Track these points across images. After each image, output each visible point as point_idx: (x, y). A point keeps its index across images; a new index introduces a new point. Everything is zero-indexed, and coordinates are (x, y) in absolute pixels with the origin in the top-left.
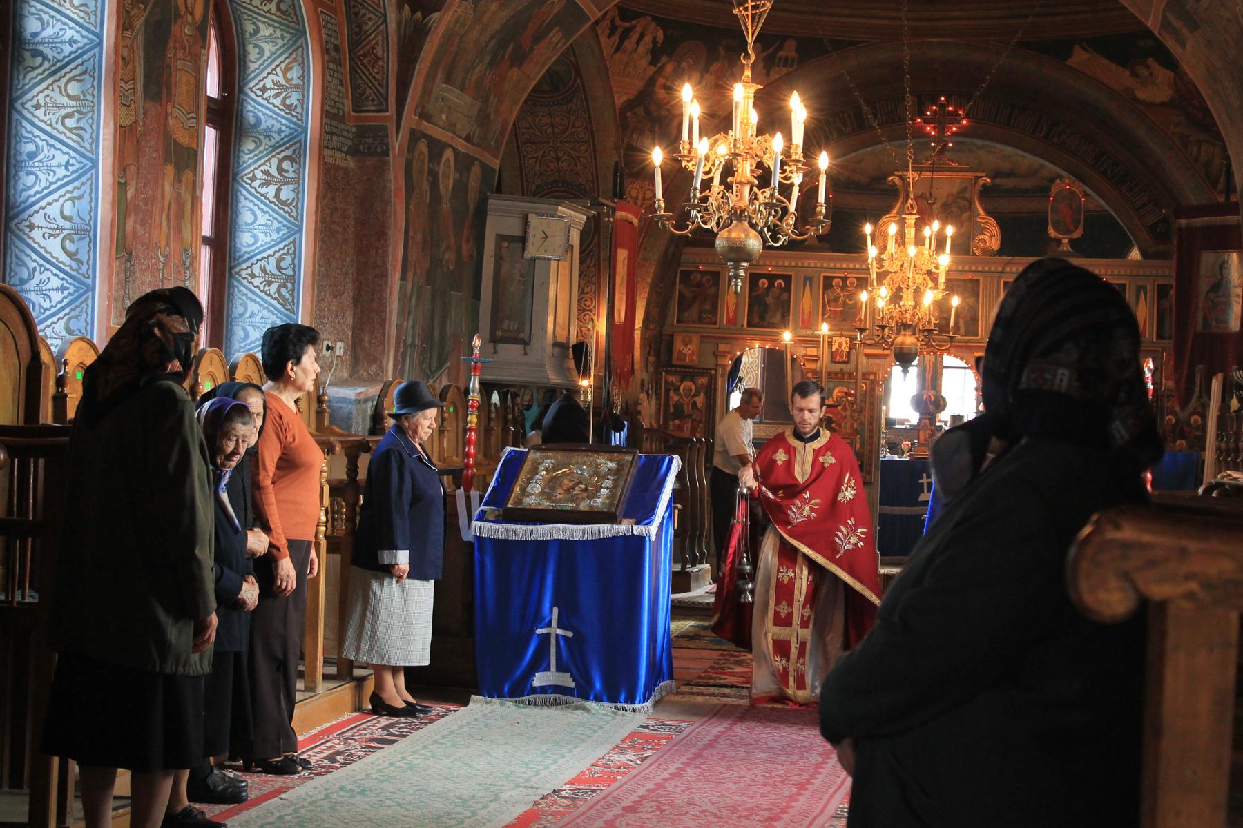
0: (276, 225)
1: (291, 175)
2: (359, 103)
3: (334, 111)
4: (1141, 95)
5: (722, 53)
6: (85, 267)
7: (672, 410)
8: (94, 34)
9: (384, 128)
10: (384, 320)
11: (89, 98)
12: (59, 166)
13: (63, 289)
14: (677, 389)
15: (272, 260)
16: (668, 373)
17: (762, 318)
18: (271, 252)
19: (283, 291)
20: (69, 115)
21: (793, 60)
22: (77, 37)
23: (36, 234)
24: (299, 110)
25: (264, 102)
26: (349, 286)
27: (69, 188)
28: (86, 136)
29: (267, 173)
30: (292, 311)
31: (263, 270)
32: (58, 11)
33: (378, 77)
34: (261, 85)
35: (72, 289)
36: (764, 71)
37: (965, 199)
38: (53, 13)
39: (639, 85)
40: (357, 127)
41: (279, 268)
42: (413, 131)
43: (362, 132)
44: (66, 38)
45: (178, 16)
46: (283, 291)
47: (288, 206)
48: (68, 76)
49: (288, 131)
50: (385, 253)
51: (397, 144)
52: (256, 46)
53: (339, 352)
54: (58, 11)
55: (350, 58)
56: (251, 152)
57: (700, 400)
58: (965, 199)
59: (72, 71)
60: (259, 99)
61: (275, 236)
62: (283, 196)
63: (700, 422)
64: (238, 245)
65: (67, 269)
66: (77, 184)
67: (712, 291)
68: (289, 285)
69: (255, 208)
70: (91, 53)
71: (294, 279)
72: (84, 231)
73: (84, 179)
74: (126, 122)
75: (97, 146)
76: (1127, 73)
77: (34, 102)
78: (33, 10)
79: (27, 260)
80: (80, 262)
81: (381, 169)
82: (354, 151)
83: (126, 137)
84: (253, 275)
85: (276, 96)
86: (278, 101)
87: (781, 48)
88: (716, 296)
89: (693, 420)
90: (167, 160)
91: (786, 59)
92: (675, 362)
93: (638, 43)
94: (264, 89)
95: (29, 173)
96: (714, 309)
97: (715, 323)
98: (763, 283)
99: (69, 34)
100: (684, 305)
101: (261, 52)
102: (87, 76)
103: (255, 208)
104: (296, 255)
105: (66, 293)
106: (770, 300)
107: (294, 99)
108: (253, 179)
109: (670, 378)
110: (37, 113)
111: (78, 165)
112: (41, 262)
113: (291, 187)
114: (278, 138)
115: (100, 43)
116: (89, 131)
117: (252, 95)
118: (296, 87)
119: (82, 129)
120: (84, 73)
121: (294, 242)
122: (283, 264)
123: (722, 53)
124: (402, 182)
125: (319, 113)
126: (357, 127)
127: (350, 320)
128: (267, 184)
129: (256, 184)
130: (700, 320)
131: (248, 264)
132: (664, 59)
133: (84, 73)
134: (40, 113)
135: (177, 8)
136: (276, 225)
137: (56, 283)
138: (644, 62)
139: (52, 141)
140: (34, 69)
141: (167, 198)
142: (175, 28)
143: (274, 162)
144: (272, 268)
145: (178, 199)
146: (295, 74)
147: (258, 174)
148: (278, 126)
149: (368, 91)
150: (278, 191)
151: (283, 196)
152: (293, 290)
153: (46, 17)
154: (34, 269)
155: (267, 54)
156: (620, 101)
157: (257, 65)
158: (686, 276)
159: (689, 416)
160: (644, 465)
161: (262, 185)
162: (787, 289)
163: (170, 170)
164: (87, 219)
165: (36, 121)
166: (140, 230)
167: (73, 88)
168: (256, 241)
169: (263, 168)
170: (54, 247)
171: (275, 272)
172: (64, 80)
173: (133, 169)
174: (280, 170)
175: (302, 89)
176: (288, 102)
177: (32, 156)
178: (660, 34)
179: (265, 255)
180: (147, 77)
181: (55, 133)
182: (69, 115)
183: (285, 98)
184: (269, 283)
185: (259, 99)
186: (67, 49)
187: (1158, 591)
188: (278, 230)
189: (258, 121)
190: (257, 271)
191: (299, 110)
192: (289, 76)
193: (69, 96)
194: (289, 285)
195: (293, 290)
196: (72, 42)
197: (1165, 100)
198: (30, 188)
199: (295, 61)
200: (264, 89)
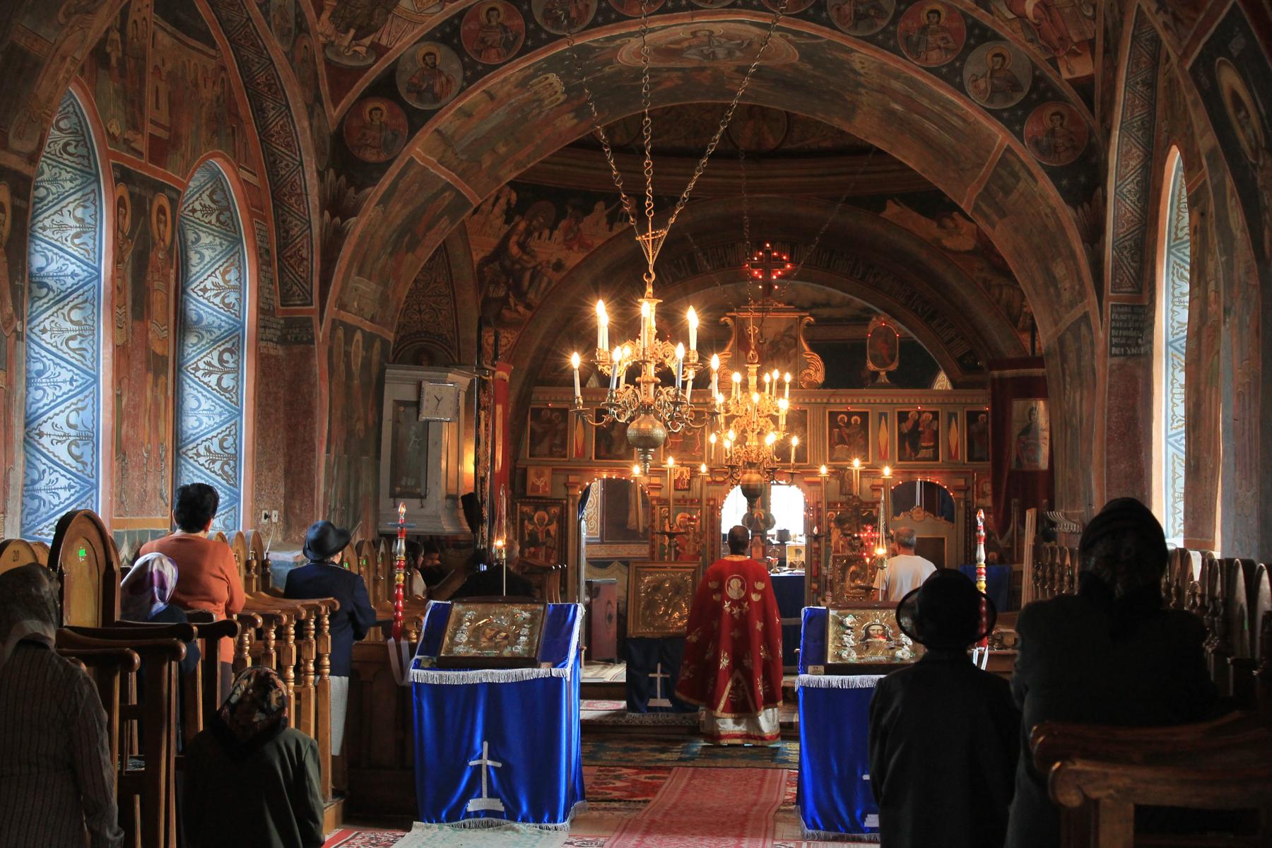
0: (218, 409)
1: (231, 365)
2: (286, 299)
3: (266, 307)
4: (948, 243)
5: (570, 211)
6: (89, 468)
7: (527, 538)
8: (93, 268)
9: (310, 320)
10: (313, 490)
11: (90, 323)
12: (65, 382)
13: (70, 487)
14: (531, 519)
15: (216, 441)
16: (522, 504)
17: (609, 450)
18: (214, 433)
19: (226, 468)
20: (73, 338)
22: (78, 271)
23: (45, 441)
24: (237, 308)
25: (205, 301)
26: (281, 460)
27: (74, 400)
28: (88, 356)
29: (209, 364)
30: (235, 486)
31: (207, 449)
32: (61, 249)
33: (304, 275)
34: (202, 286)
35: (78, 488)
37: (791, 337)
38: (56, 250)
39: (495, 241)
40: (285, 319)
41: (222, 448)
42: (334, 321)
43: (290, 323)
44: (69, 272)
45: (154, 244)
46: (226, 468)
47: (229, 392)
48: (71, 304)
49: (227, 327)
50: (313, 430)
51: (320, 334)
52: (197, 252)
53: (275, 519)
54: (61, 249)
55: (279, 259)
56: (194, 345)
57: (553, 528)
58: (791, 337)
59: (74, 300)
60: (201, 299)
61: (218, 419)
62: (224, 384)
64: (185, 428)
65: (74, 470)
66: (80, 397)
67: (561, 427)
68: (232, 462)
69: (199, 395)
70: (90, 285)
71: (236, 457)
72: (88, 437)
73: (86, 393)
74: (120, 342)
75: (98, 365)
76: (935, 225)
77: (41, 327)
78: (38, 248)
79: (37, 463)
80: (84, 464)
81: (307, 356)
82: (282, 341)
83: (122, 354)
84: (198, 455)
85: (216, 295)
86: (217, 300)
88: (566, 429)
90: (148, 370)
92: (529, 493)
93: (494, 205)
94: (205, 290)
95: (37, 388)
96: (564, 445)
97: (565, 456)
99: (71, 268)
100: (536, 440)
101: (202, 257)
102: (87, 305)
103: (199, 395)
104: (237, 436)
105: (73, 491)
107: (232, 298)
108: (197, 369)
109: (525, 509)
110: (44, 336)
111: (81, 381)
112: (50, 464)
113: (232, 376)
114: (218, 333)
115: (99, 277)
116: (91, 351)
117: (194, 295)
118: (234, 288)
119: (84, 349)
120: (85, 301)
121: (235, 424)
122: (225, 445)
123: (570, 211)
124: (326, 367)
125: (255, 310)
126: (285, 319)
127: (282, 490)
128: (210, 373)
129: (199, 374)
130: (551, 454)
131: (194, 444)
132: (517, 219)
133: (85, 301)
134: (46, 336)
135: (153, 238)
136: (218, 409)
137: (63, 482)
138: (499, 222)
139: (58, 361)
140: (40, 298)
141: (149, 401)
142: (151, 254)
143: (216, 354)
144: (215, 448)
145: (155, 398)
146: (232, 276)
147: (201, 365)
148: (218, 322)
149: (295, 288)
150: (220, 380)
151: (224, 384)
152: (235, 467)
153: (50, 254)
154: (44, 471)
155: (207, 259)
156: (477, 258)
157: (198, 269)
158: (537, 413)
159: (544, 544)
160: (553, 612)
161: (205, 375)
163: (150, 377)
164: (90, 426)
165: (43, 343)
166: (131, 433)
167: (76, 315)
168: (201, 424)
169: (205, 359)
170: (61, 451)
171: (219, 451)
172: (67, 308)
173: (126, 381)
174: (221, 361)
175: (239, 289)
176: (227, 301)
177: (40, 373)
178: (514, 196)
179: (209, 436)
180: (134, 301)
181: (60, 353)
182: (73, 338)
183: (224, 298)
184: (214, 462)
185: (201, 299)
186: (70, 281)
187: (1095, 794)
188: (220, 414)
189: (200, 318)
190: (202, 451)
191: (237, 308)
192: (227, 277)
193: (72, 322)
194: (232, 462)
195: (235, 467)
196: (73, 275)
198: (39, 401)
199: (232, 264)
200: (205, 290)
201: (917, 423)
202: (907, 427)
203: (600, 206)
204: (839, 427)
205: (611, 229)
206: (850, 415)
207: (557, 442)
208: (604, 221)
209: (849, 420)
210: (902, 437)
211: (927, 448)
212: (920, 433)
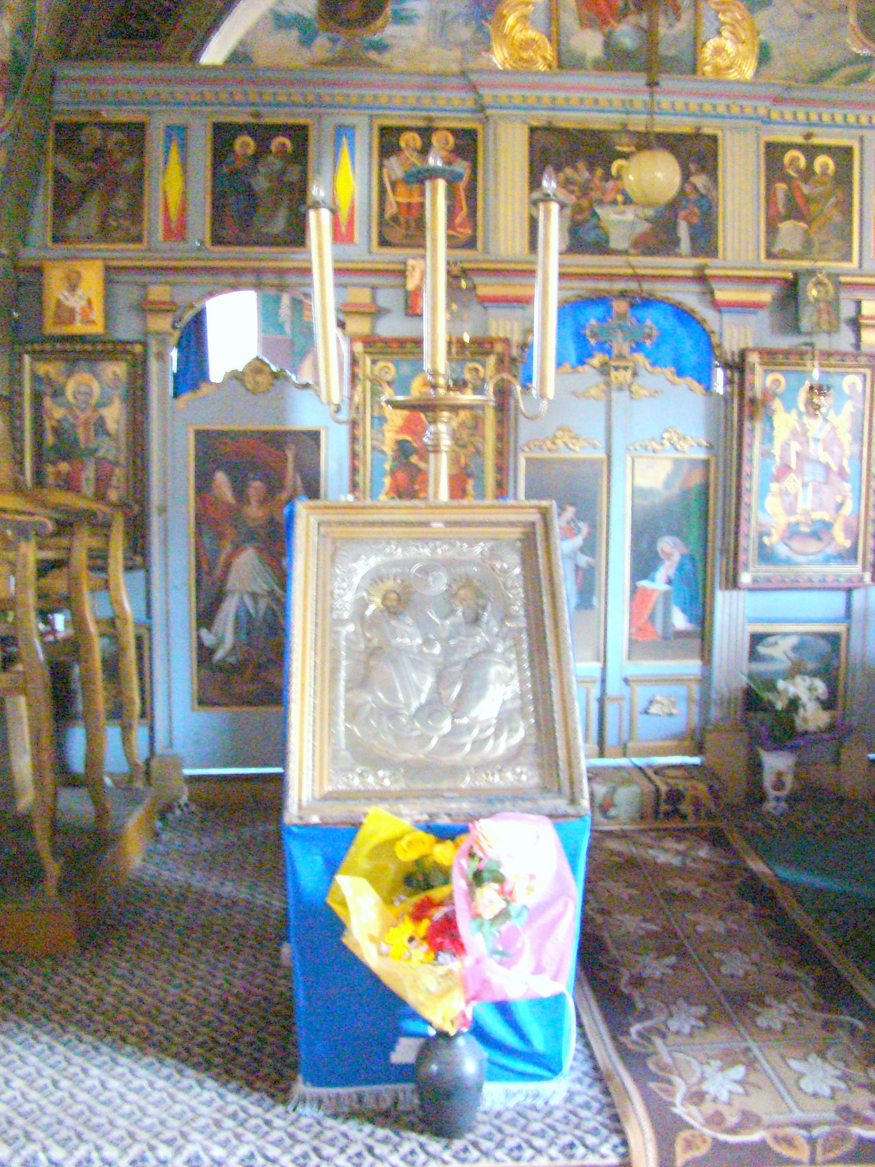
7: (50, 439)
14: (58, 393)
16: (39, 356)
17: (247, 224)
63: (116, 464)
67: (130, 167)
89: (99, 461)
92: (51, 328)
96: (135, 212)
97: (138, 239)
98: (245, 144)
106: (261, 183)
109: (43, 368)
130: (105, 233)
204: (786, 179)
206: (811, 152)
207: (121, 202)
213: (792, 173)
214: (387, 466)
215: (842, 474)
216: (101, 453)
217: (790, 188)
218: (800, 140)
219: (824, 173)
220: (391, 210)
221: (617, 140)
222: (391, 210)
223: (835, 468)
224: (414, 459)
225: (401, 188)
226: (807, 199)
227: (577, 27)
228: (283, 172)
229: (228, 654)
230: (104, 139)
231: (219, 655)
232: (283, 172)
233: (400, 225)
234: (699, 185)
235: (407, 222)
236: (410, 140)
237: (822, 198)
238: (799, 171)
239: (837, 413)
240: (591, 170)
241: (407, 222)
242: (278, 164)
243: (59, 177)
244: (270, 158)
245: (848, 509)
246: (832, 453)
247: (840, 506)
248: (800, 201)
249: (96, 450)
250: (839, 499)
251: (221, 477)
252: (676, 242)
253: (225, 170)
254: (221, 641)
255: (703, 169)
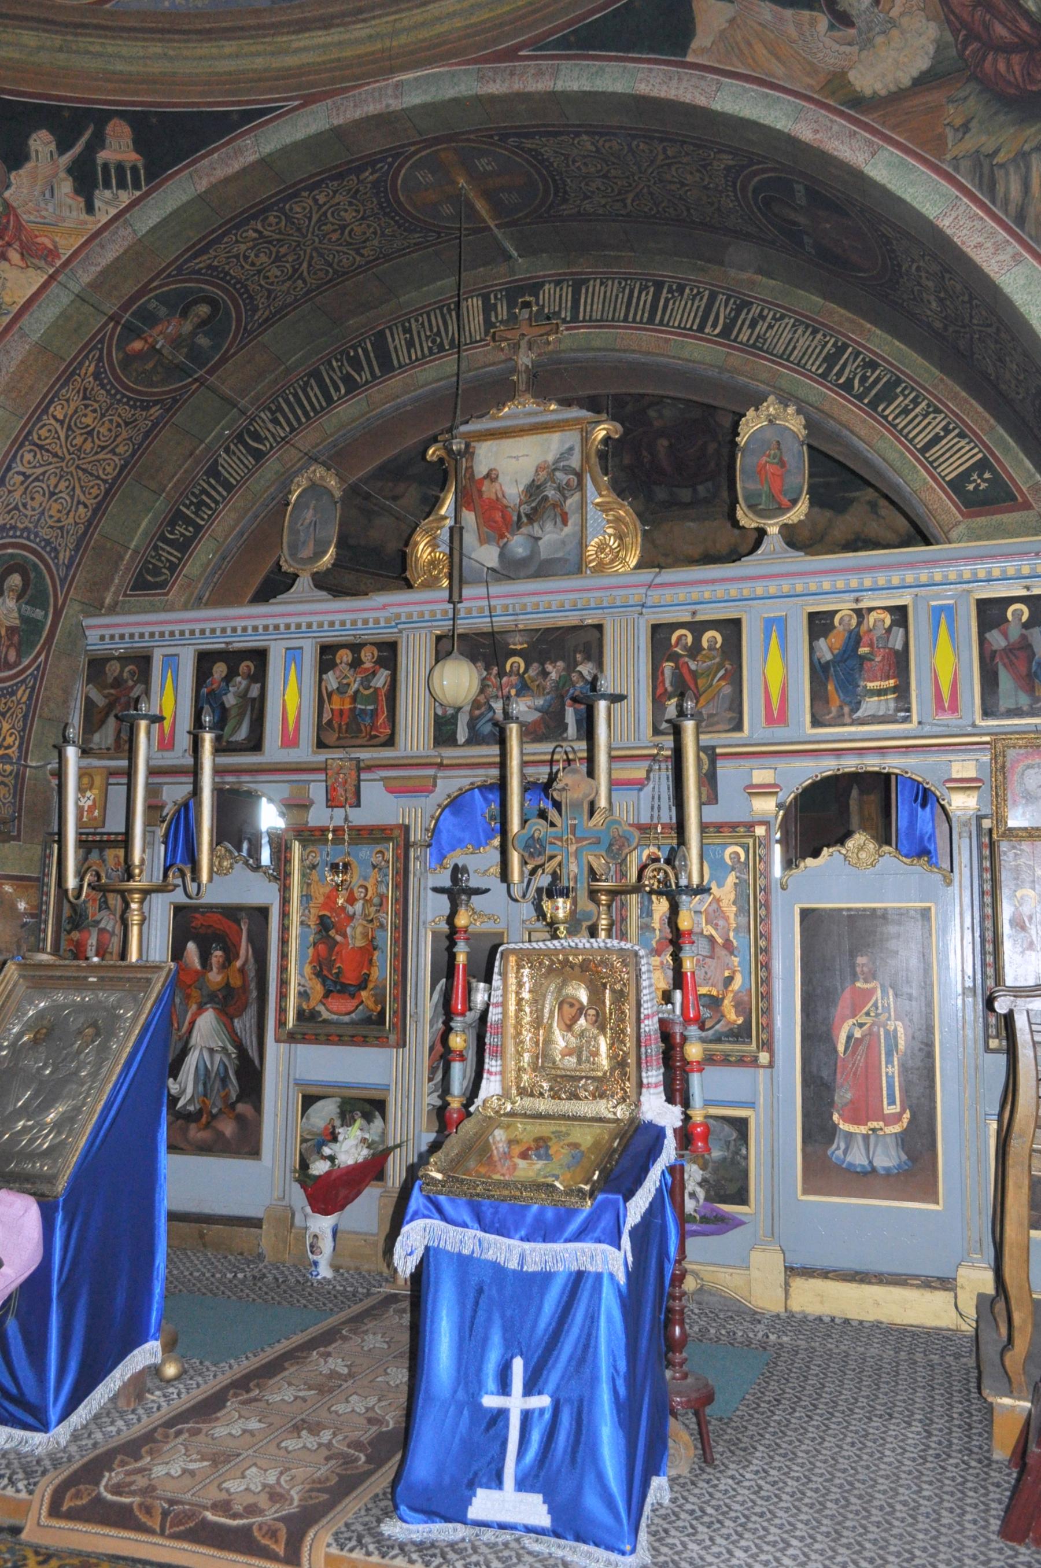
4: (870, 78)
21: (134, 169)
36: (81, 201)
37: (567, 470)
58: (567, 470)
76: (823, 21)
87: (98, 141)
91: (120, 168)
98: (220, 670)
106: (230, 700)
162: (260, 676)
197: (923, 64)
201: (855, 639)
202: (826, 649)
203: (41, 143)
204: (674, 657)
205: (90, 209)
206: (698, 628)
208: (67, 187)
209: (697, 639)
210: (819, 672)
211: (880, 692)
212: (863, 658)
213: (678, 650)
214: (311, 939)
215: (728, 945)
216: (102, 925)
217: (677, 667)
218: (688, 618)
219: (711, 648)
220: (327, 717)
221: (511, 640)
222: (327, 717)
223: (720, 941)
224: (332, 933)
225: (335, 698)
226: (694, 674)
227: (476, 543)
228: (247, 690)
229: (191, 1101)
230: (122, 671)
231: (180, 1104)
232: (247, 690)
233: (333, 729)
234: (585, 673)
235: (340, 726)
236: (345, 656)
237: (711, 672)
238: (685, 648)
239: (720, 885)
240: (487, 668)
241: (340, 726)
242: (244, 683)
243: (89, 703)
244: (239, 679)
245: (737, 984)
246: (716, 927)
247: (730, 980)
248: (688, 677)
249: (99, 922)
250: (727, 974)
251: (191, 946)
252: (565, 727)
253: (204, 691)
254: (183, 1092)
255: (588, 658)
